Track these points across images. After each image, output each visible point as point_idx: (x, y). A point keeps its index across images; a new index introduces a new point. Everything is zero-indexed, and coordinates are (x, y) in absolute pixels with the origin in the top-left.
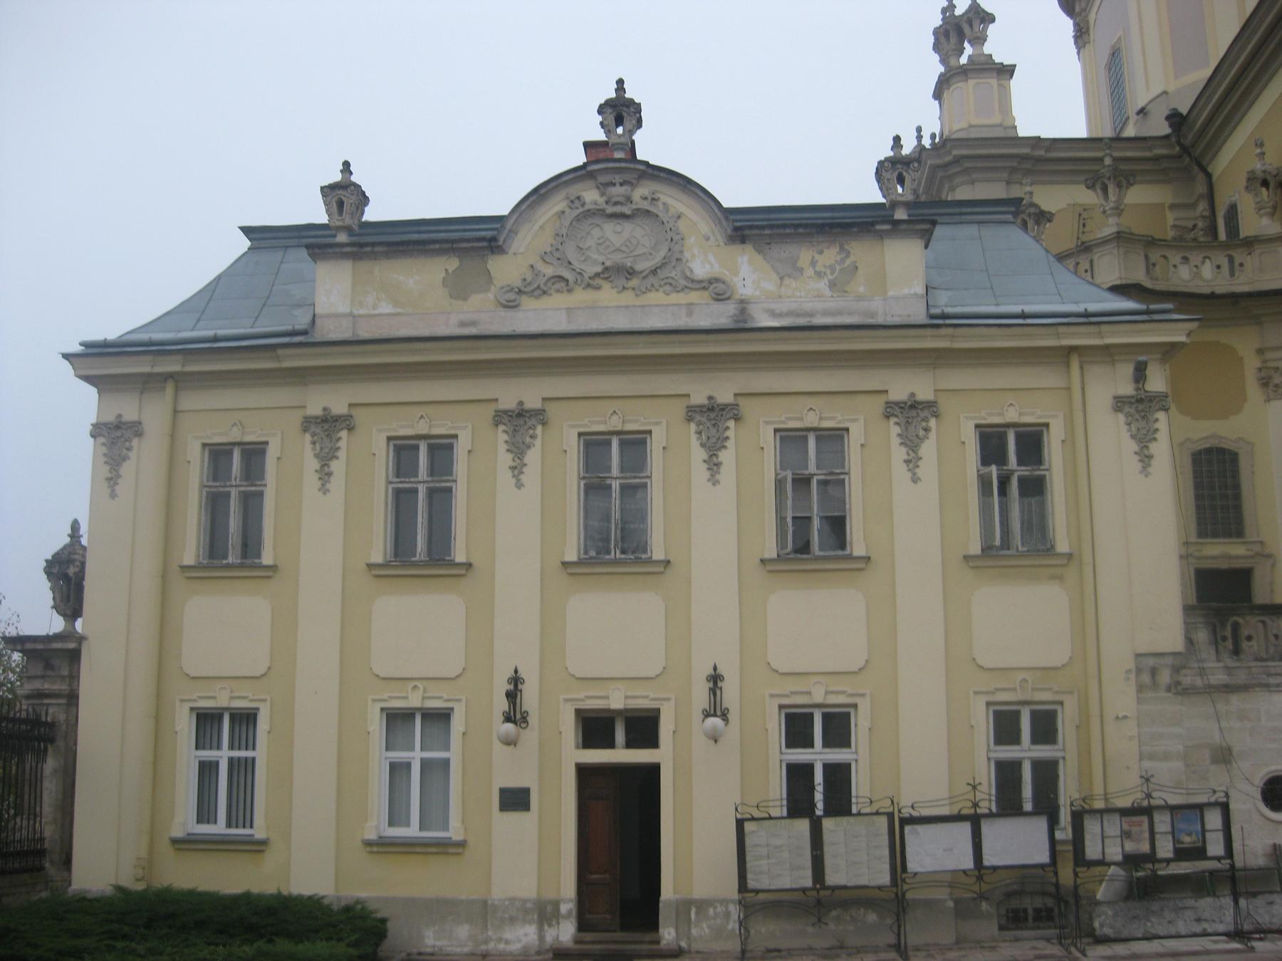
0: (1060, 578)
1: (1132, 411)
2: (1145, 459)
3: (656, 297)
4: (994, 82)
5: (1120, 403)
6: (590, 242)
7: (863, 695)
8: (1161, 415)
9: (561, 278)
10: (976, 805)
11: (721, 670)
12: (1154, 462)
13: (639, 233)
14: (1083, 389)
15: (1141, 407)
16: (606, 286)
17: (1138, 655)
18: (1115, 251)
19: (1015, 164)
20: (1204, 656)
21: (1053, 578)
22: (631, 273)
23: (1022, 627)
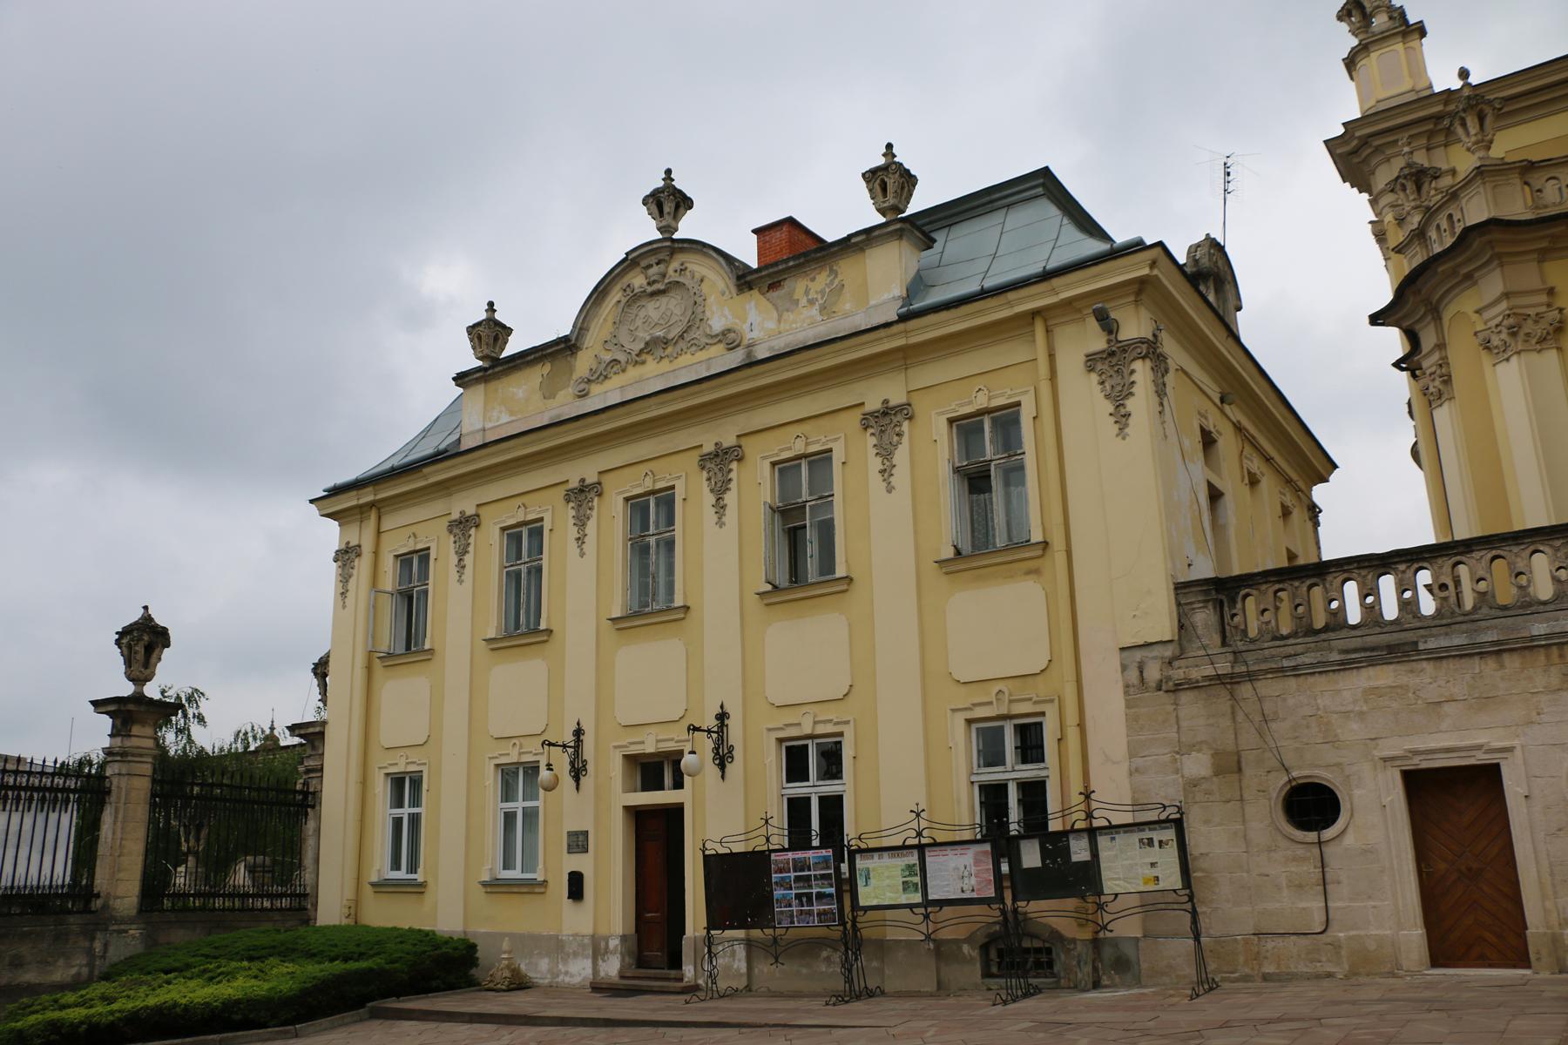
0: (1036, 572)
1: (1106, 367)
2: (1122, 418)
3: (685, 359)
4: (1399, 47)
5: (1092, 361)
6: (639, 322)
7: (847, 722)
8: (1138, 365)
9: (615, 361)
10: (919, 834)
11: (727, 709)
12: (1131, 421)
13: (673, 302)
14: (1052, 357)
15: (1114, 361)
16: (649, 358)
17: (1122, 649)
18: (1481, 189)
19: (1431, 126)
20: (1205, 641)
21: (1029, 572)
22: (666, 342)
23: (999, 632)
